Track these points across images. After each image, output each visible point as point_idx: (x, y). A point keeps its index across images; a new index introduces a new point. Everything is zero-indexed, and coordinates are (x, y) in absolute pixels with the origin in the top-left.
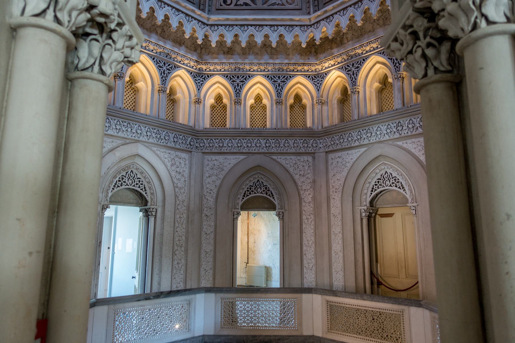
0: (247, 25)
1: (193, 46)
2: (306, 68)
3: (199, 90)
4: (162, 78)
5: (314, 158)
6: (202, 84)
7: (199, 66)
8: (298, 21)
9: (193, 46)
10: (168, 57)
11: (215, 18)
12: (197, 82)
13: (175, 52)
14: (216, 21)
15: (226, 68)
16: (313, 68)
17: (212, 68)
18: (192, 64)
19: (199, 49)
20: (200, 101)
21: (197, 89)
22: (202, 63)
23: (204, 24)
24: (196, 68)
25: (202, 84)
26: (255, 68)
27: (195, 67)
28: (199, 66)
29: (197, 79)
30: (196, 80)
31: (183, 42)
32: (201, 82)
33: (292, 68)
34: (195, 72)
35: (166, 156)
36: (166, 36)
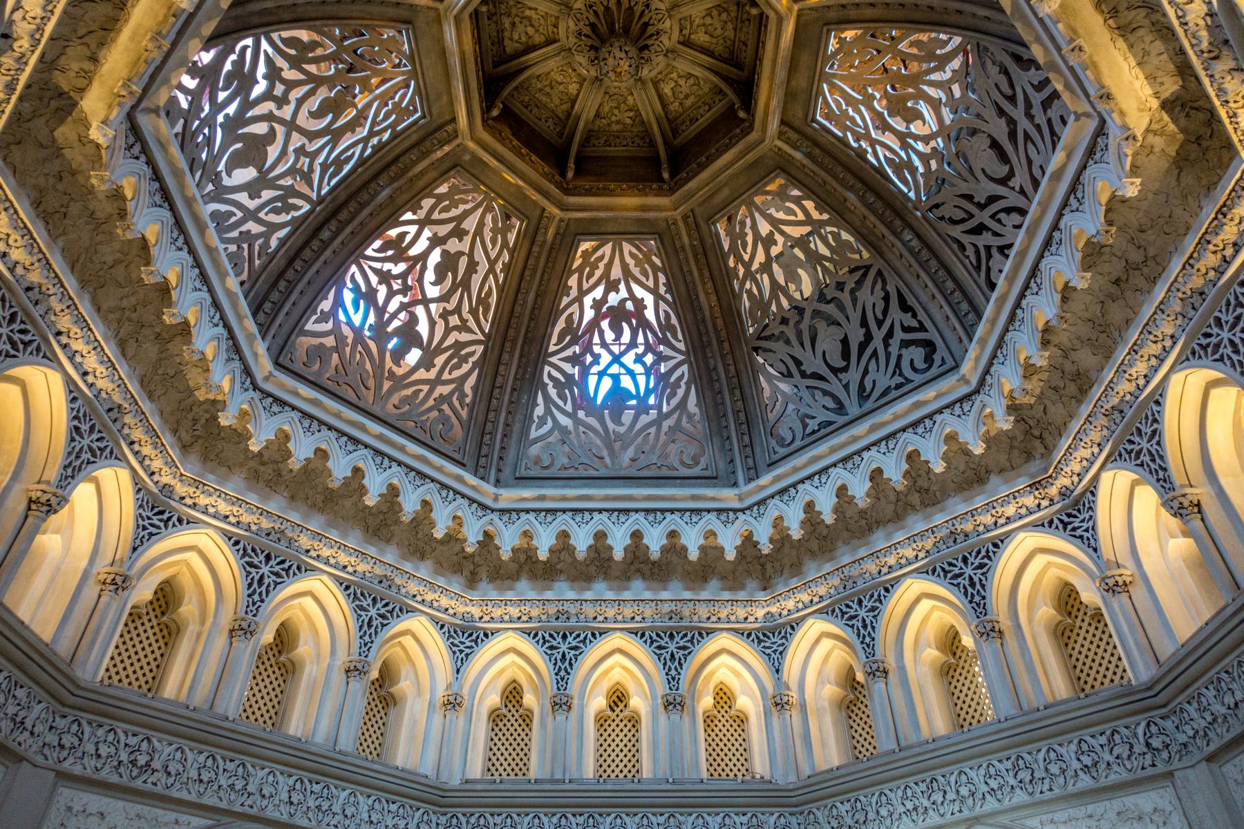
1: (1016, 451)
3: (1095, 550)
4: (971, 602)
7: (1053, 491)
8: (1069, 156)
9: (1016, 451)
10: (960, 538)
12: (1079, 532)
14: (975, 368)
18: (1030, 501)
19: (1037, 443)
21: (1091, 551)
22: (1050, 476)
24: (1051, 500)
26: (1141, 368)
27: (1045, 503)
28: (1053, 491)
29: (1076, 525)
30: (1074, 529)
31: (983, 470)
32: (1091, 524)
33: (1211, 260)
34: (1058, 511)
36: (938, 494)
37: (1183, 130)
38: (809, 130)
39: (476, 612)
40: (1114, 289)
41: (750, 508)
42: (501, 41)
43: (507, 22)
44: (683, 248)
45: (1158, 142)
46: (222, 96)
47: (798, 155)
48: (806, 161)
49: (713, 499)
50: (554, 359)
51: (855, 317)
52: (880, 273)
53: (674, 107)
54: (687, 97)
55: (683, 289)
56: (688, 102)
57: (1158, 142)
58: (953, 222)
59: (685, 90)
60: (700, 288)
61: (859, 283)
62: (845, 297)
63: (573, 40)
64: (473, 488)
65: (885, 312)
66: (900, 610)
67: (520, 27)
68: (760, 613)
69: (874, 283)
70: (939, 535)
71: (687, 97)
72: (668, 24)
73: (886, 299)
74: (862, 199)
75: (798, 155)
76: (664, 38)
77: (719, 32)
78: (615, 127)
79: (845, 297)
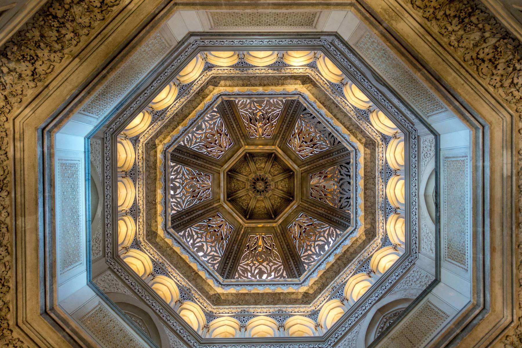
0: (334, 128)
2: (317, 77)
7: (380, 143)
16: (313, 73)
17: (374, 134)
35: (423, 163)
37: (309, 83)
38: (304, 162)
39: (313, 308)
41: (356, 226)
42: (243, 208)
43: (241, 204)
44: (308, 207)
45: (310, 88)
46: (188, 240)
47: (306, 167)
48: (308, 166)
49: (347, 233)
50: (302, 255)
51: (345, 177)
52: (341, 166)
53: (285, 189)
55: (317, 215)
56: (287, 186)
57: (310, 88)
59: (284, 184)
60: (318, 210)
61: (340, 172)
63: (253, 194)
64: (291, 281)
66: (394, 198)
67: (244, 202)
68: (379, 241)
70: (379, 176)
73: (345, 167)
74: (323, 159)
75: (306, 167)
76: (269, 178)
78: (279, 205)
79: (342, 177)
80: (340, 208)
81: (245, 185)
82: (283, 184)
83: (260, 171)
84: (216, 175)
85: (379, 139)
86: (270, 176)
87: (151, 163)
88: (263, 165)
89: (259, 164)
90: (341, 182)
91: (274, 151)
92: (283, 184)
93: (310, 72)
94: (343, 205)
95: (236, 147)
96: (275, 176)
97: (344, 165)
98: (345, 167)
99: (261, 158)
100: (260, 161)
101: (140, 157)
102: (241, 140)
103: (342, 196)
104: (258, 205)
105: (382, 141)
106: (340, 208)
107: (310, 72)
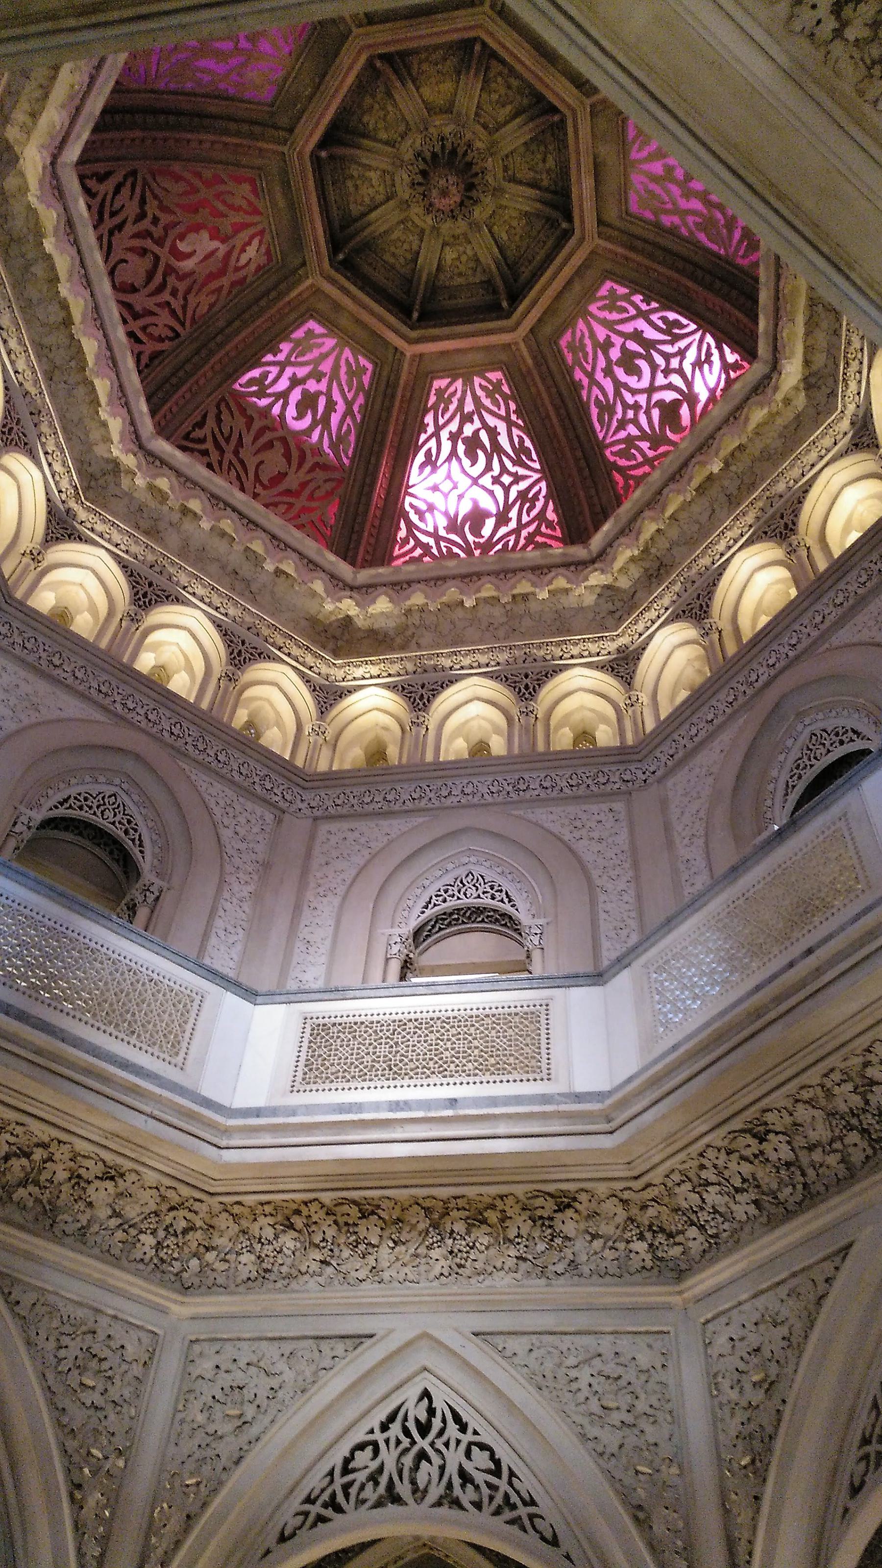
5: (279, 821)
6: (57, 538)
11: (163, 447)
13: (51, 425)
15: (134, 549)
17: (99, 527)
20: (40, 558)
23: (138, 437)
25: (57, 538)
26: (200, 591)
40: (230, 569)
52: (178, 335)
54: (356, 187)
56: (349, 183)
58: (219, 421)
61: (173, 313)
62: (166, 296)
63: (469, 136)
65: (151, 336)
67: (503, 91)
69: (172, 329)
71: (356, 187)
72: (430, 222)
73: (161, 339)
77: (393, 249)
80: (134, 173)
81: (506, 169)
82: (367, 193)
83: (458, 232)
84: (612, 214)
85: (82, 515)
86: (417, 220)
87: (824, 325)
88: (450, 255)
89: (464, 258)
90: (158, 279)
91: (414, 334)
92: (367, 193)
93: (332, 671)
94: (126, 191)
95: (548, 329)
96: (402, 222)
97: (166, 345)
98: (161, 339)
99: (459, 281)
100: (462, 268)
101: (854, 365)
102: (530, 361)
103: (145, 224)
104: (447, 86)
105: (68, 511)
106: (134, 173)
107: (332, 671)
